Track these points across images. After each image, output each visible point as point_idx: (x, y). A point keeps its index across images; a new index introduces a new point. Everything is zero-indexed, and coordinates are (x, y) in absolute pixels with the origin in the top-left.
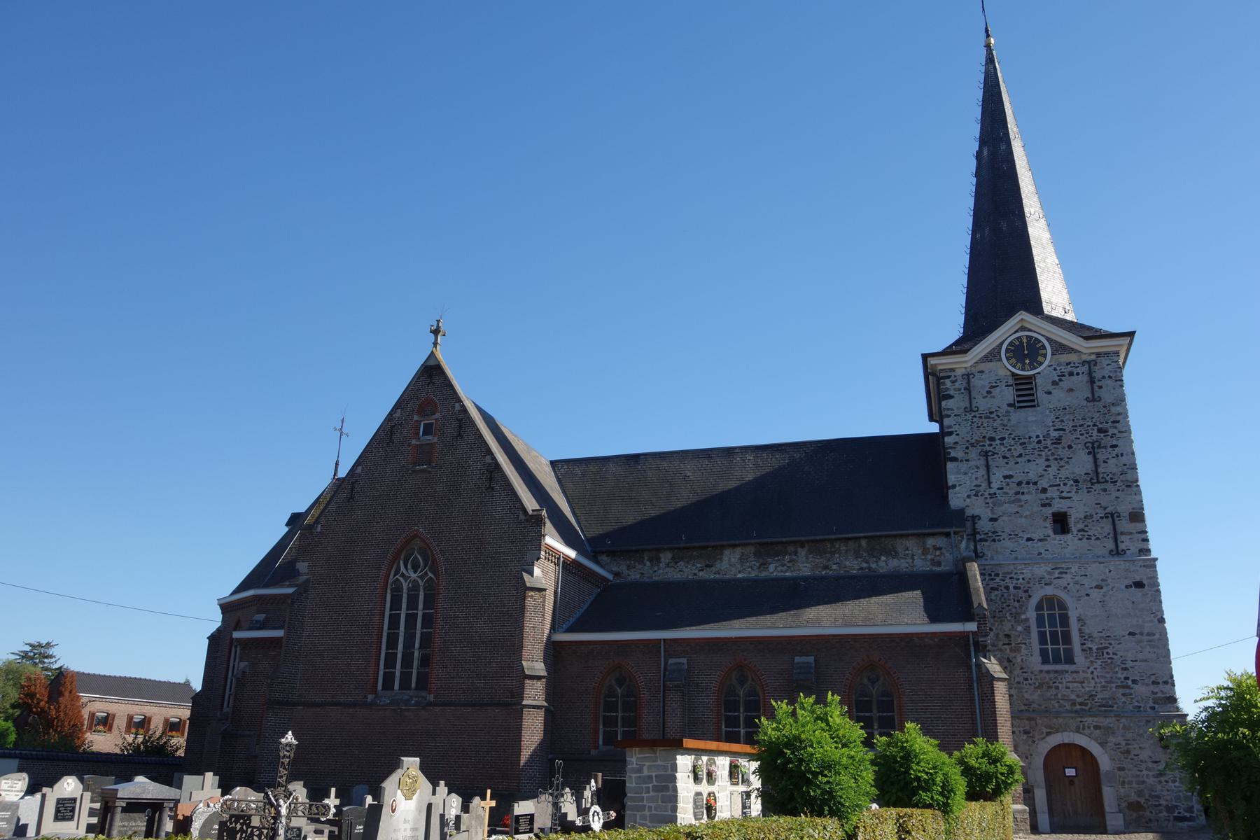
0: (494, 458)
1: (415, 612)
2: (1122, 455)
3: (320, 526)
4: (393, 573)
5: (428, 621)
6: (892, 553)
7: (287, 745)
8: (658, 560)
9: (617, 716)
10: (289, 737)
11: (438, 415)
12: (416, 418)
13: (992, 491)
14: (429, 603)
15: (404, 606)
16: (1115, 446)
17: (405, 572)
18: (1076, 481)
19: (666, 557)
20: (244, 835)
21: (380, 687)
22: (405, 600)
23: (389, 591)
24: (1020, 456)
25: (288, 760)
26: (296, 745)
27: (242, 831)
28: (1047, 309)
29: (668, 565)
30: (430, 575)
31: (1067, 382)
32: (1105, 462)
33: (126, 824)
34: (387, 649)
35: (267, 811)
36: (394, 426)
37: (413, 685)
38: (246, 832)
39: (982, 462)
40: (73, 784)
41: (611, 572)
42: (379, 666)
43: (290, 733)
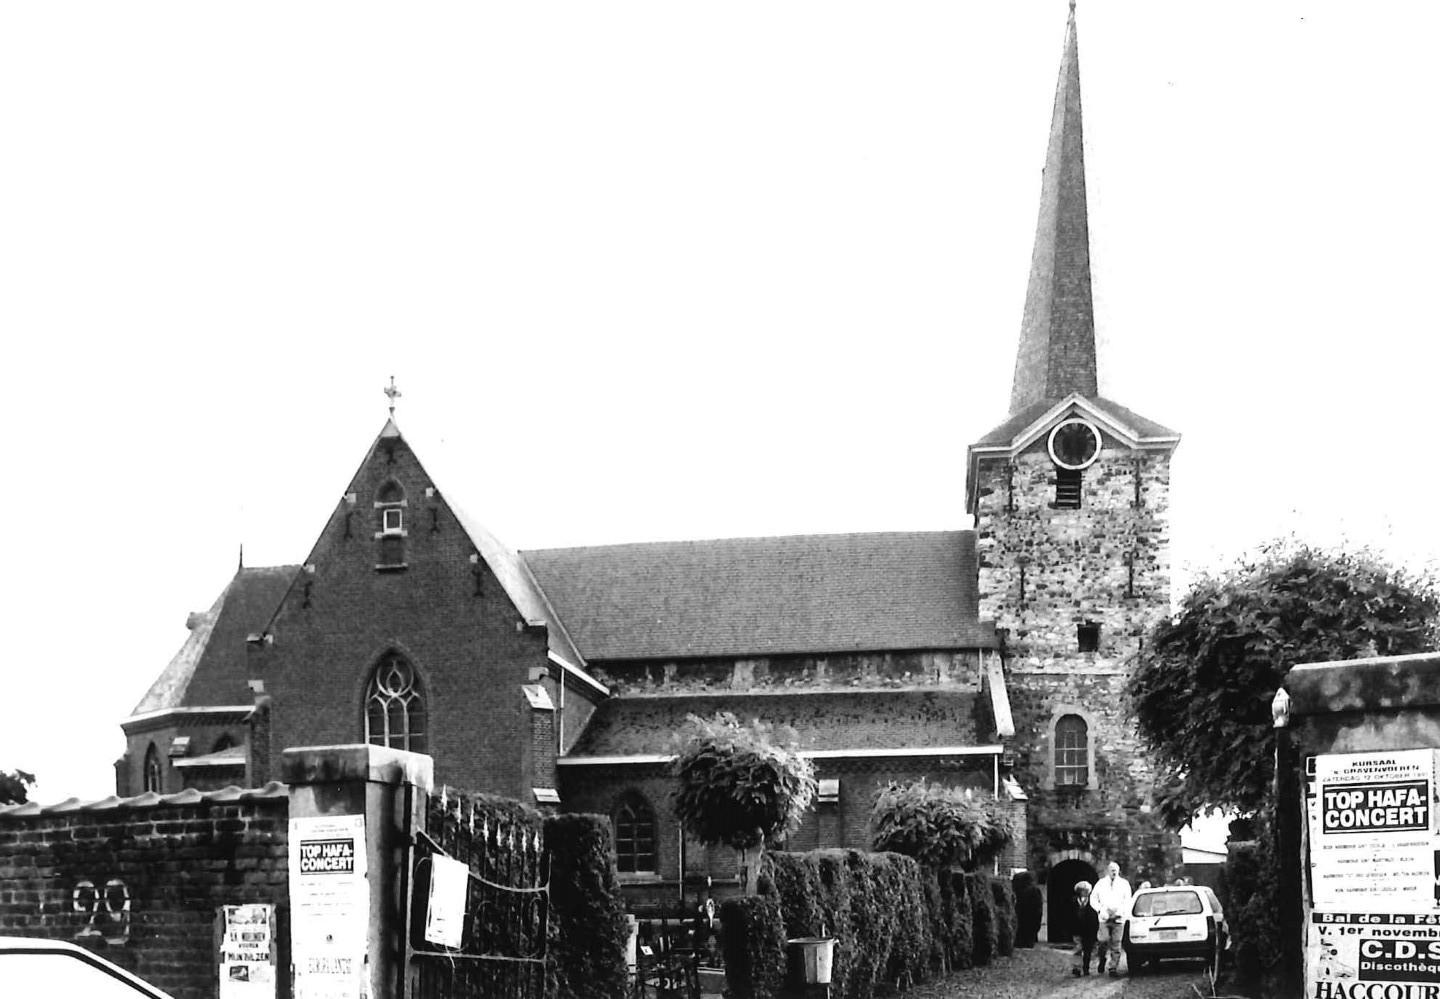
2: (1158, 568)
4: (369, 693)
6: (917, 670)
13: (1025, 601)
15: (387, 729)
16: (1154, 558)
18: (1110, 595)
24: (1057, 563)
28: (1105, 391)
31: (1113, 482)
32: (1140, 574)
39: (1017, 569)
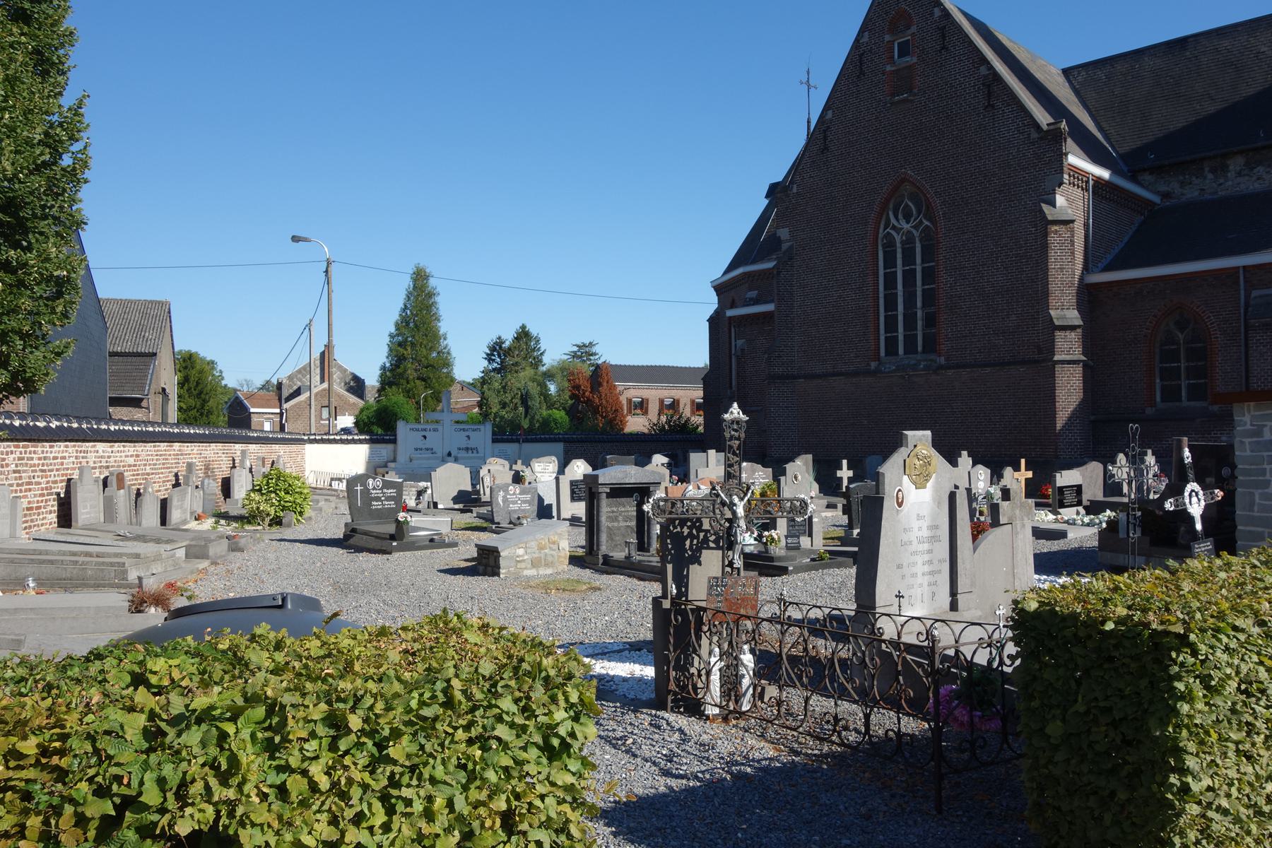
0: (991, 68)
1: (913, 267)
3: (795, 186)
4: (882, 226)
5: (929, 275)
7: (733, 422)
8: (1225, 168)
9: (1179, 367)
10: (735, 411)
11: (914, 29)
12: (887, 38)
14: (928, 253)
15: (899, 261)
17: (896, 224)
19: (1236, 163)
20: (695, 542)
21: (882, 353)
22: (899, 255)
23: (880, 248)
25: (737, 442)
26: (746, 422)
27: (690, 535)
29: (1239, 174)
30: (926, 223)
33: (615, 509)
34: (886, 311)
35: (717, 511)
36: (863, 54)
37: (920, 349)
38: (698, 537)
40: (583, 466)
41: (1157, 193)
42: (879, 331)
43: (735, 405)
